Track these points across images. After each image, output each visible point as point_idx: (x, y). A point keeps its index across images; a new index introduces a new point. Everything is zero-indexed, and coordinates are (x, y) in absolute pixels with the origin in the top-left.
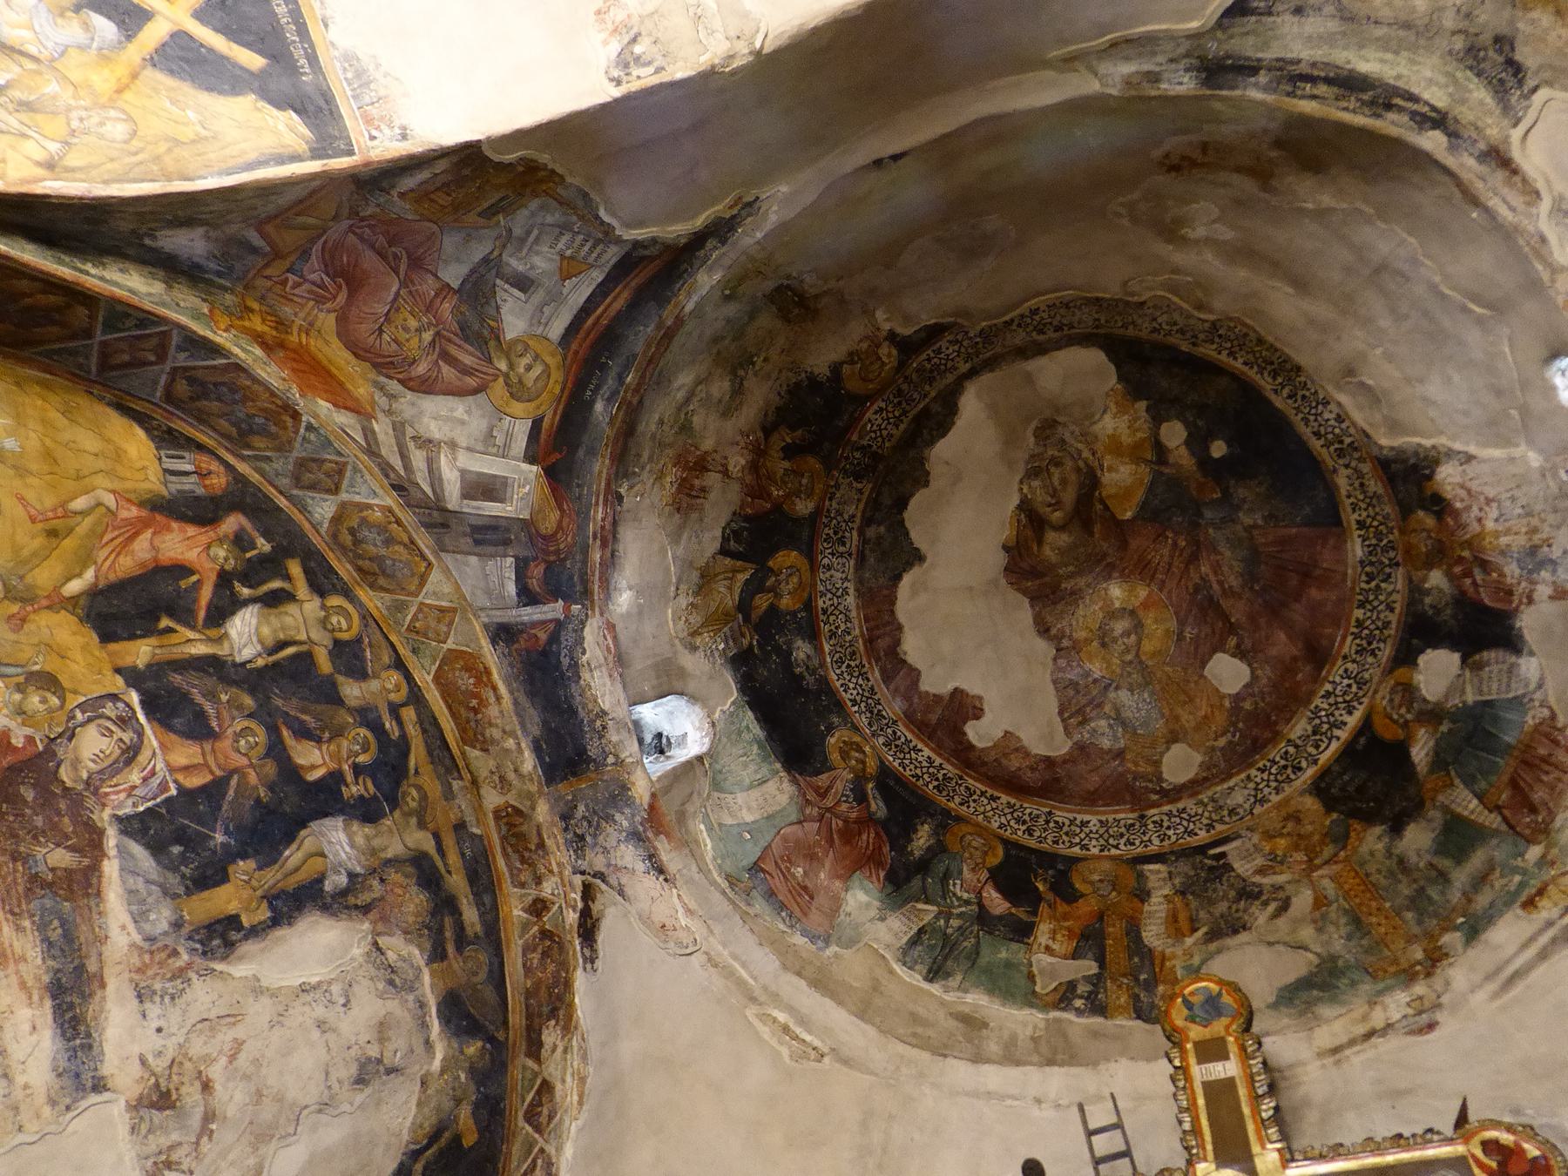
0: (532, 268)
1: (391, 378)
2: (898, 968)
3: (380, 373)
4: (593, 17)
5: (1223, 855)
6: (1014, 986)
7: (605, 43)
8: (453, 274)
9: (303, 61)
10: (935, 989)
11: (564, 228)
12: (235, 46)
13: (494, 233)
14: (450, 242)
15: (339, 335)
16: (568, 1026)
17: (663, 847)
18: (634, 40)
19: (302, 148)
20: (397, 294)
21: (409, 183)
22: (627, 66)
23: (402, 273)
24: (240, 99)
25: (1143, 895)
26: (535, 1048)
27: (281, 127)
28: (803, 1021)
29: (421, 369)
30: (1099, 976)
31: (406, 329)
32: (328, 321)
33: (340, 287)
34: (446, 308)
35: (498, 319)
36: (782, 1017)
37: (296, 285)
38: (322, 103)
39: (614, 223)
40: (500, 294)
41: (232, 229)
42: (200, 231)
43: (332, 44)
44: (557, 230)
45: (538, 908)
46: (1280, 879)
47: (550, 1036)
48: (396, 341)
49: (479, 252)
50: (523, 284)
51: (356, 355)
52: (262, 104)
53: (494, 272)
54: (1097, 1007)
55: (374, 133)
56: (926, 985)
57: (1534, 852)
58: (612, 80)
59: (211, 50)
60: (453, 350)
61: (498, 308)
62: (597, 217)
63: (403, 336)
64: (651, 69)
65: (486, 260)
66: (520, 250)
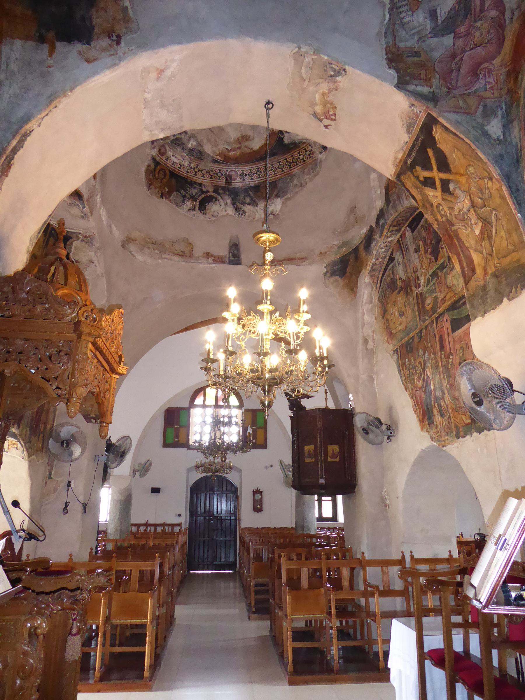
0: (425, 18)
1: (505, 20)
3: (505, 25)
4: (339, 90)
7: (340, 82)
8: (448, 40)
9: (419, 141)
11: (403, 25)
12: (431, 157)
13: (423, 44)
14: (437, 55)
15: (499, 53)
18: (332, 76)
19: (438, 126)
20: (471, 50)
21: (424, 89)
22: (339, 72)
23: (461, 57)
24: (441, 148)
27: (438, 134)
29: (493, 13)
31: (481, 34)
32: (497, 62)
33: (481, 70)
34: (462, 29)
35: (454, 6)
37: (490, 83)
38: (424, 130)
39: (387, 10)
40: (444, 17)
41: (480, 120)
42: (486, 128)
43: (409, 137)
44: (405, 26)
48: (488, 33)
49: (433, 41)
50: (433, 14)
51: (504, 40)
52: (438, 143)
53: (438, 28)
55: (419, 112)
58: (346, 72)
59: (437, 162)
60: (478, 9)
61: (449, 12)
62: (390, 19)
63: (485, 32)
64: (332, 66)
65: (435, 36)
66: (422, 30)
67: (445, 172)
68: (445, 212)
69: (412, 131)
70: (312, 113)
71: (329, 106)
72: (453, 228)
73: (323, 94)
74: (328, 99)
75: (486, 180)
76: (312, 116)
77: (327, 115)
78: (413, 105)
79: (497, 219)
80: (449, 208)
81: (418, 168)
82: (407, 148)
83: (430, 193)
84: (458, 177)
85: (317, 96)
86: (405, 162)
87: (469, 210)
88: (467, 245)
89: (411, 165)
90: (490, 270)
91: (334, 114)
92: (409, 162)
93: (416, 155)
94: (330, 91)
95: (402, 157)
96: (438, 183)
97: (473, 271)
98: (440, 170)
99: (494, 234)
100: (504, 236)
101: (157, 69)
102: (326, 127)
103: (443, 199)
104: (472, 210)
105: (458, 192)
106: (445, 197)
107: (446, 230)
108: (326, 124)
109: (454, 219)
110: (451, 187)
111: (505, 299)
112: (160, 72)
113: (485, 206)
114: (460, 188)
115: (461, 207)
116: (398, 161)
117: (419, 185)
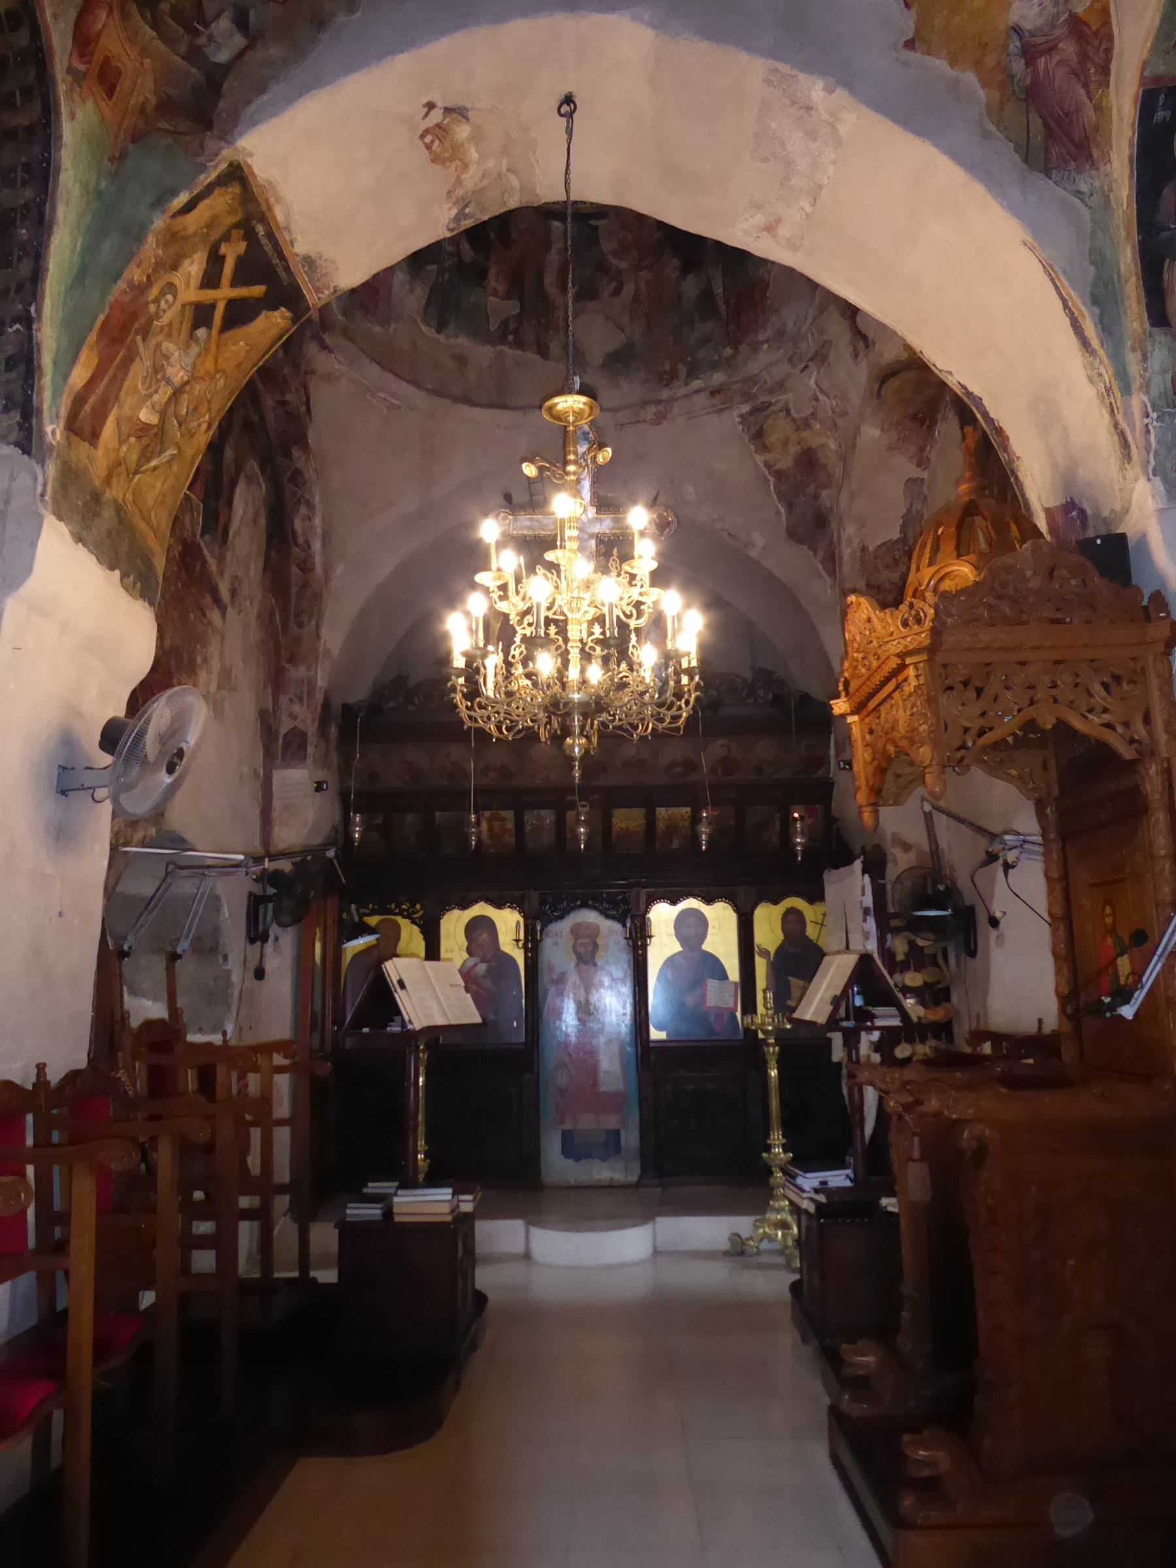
2: (424, 328)
5: (596, 228)
6: (478, 330)
7: (450, 209)
10: (442, 337)
16: (305, 447)
17: (327, 339)
18: (466, 206)
25: (547, 245)
26: (289, 456)
27: (279, 320)
28: (392, 395)
30: (519, 315)
36: (382, 395)
45: (284, 403)
46: (624, 265)
47: (296, 452)
54: (519, 344)
56: (436, 335)
57: (728, 352)
67: (224, 317)
68: (164, 311)
69: (304, 267)
70: (470, 114)
71: (447, 155)
72: (139, 338)
73: (466, 166)
74: (453, 166)
75: (207, 417)
76: (468, 106)
77: (437, 131)
78: (335, 292)
79: (169, 463)
80: (170, 325)
81: (242, 247)
82: (283, 237)
83: (194, 266)
84: (213, 350)
85: (475, 155)
86: (263, 219)
87: (169, 382)
88: (123, 394)
89: (253, 229)
90: (117, 492)
91: (428, 147)
92: (260, 229)
93: (265, 252)
94: (459, 182)
95: (275, 217)
96: (210, 295)
97: (94, 437)
98: (231, 304)
99: (153, 463)
100: (157, 491)
101: (774, 236)
102: (431, 106)
103: (184, 306)
104: (170, 391)
105: (195, 349)
106: (187, 313)
107: (134, 316)
108: (433, 112)
109: (153, 342)
110: (201, 332)
111: (117, 573)
112: (769, 229)
113: (180, 425)
114: (199, 355)
115: (172, 360)
116: (272, 200)
117: (216, 234)
